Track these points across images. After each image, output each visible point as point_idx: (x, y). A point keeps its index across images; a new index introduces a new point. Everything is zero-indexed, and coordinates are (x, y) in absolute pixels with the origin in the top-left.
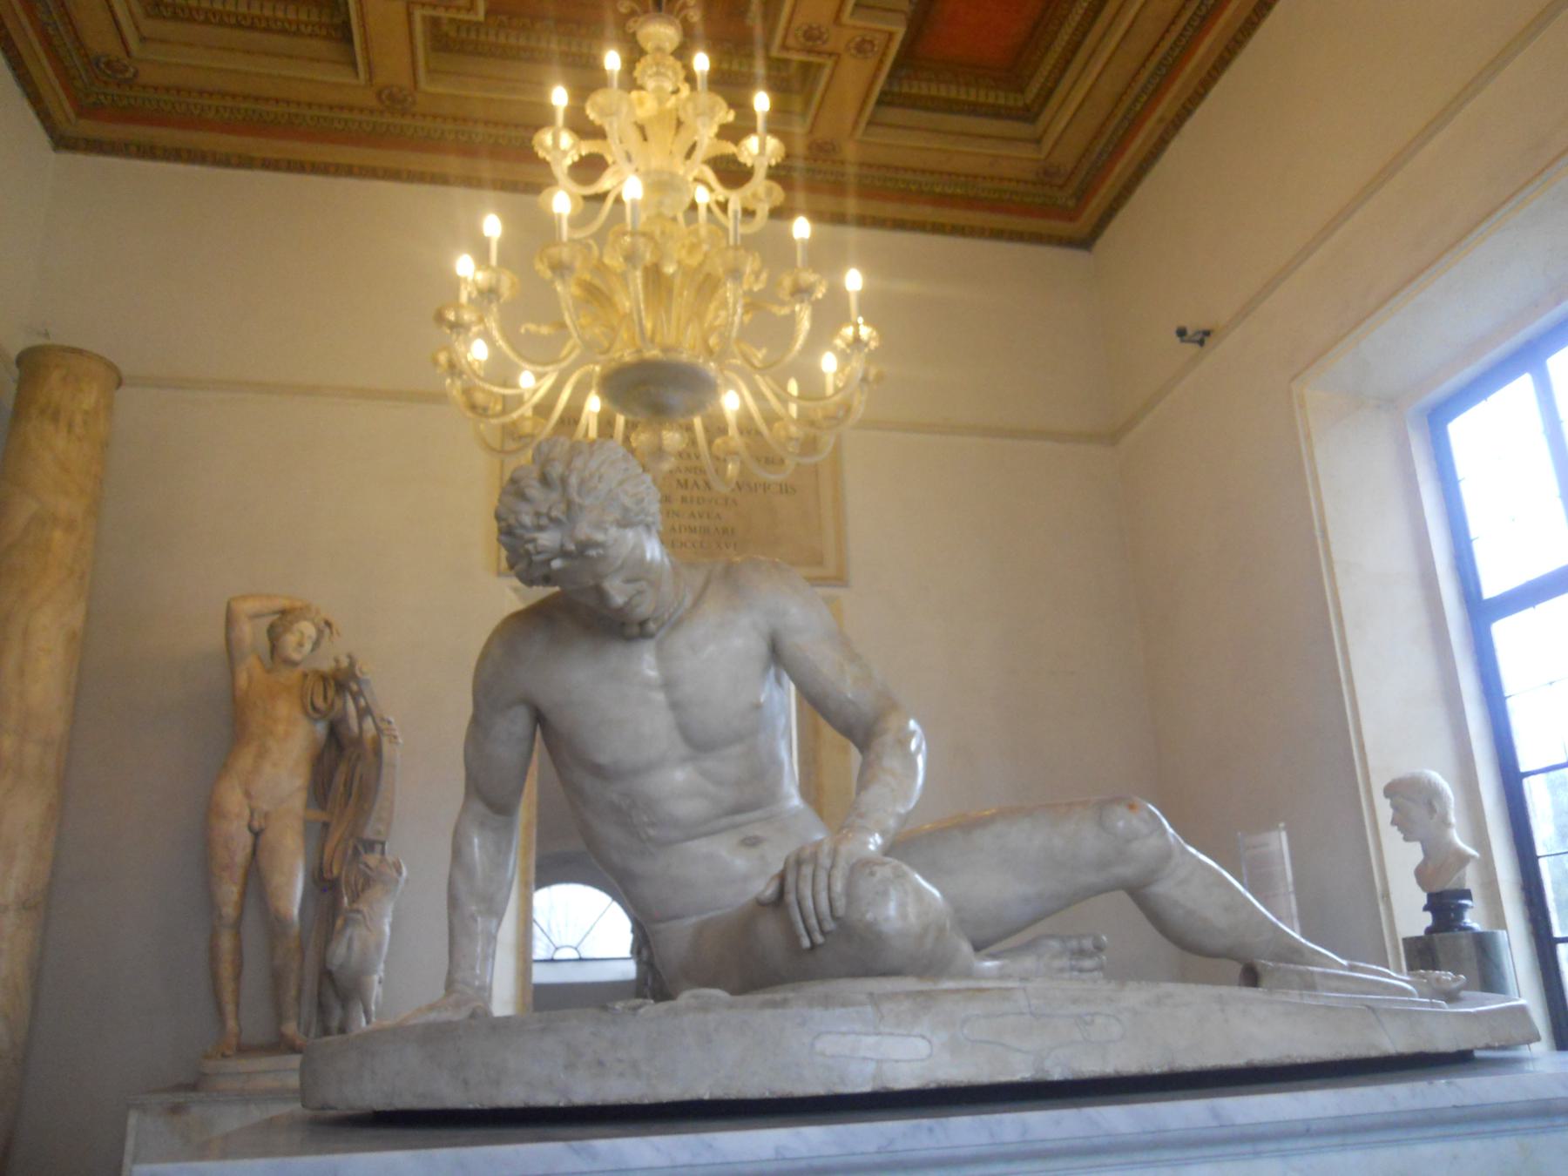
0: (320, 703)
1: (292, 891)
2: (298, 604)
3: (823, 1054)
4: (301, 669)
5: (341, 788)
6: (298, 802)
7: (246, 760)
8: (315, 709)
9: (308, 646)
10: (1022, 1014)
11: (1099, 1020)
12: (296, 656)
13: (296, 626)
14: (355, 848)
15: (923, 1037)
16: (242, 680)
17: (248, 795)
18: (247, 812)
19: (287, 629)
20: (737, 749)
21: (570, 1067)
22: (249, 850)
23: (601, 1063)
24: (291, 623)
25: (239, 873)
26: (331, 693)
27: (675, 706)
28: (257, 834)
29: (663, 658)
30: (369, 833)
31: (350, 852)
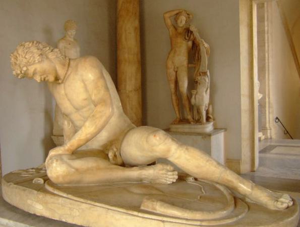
0: (187, 38)
1: (184, 85)
2: (181, 11)
4: (185, 27)
6: (185, 63)
7: (172, 54)
8: (186, 39)
11: (75, 210)
12: (181, 25)
15: (42, 204)
16: (171, 34)
17: (173, 63)
18: (173, 67)
20: (85, 109)
22: (175, 76)
25: (173, 81)
26: (189, 34)
28: (176, 72)
29: (65, 89)
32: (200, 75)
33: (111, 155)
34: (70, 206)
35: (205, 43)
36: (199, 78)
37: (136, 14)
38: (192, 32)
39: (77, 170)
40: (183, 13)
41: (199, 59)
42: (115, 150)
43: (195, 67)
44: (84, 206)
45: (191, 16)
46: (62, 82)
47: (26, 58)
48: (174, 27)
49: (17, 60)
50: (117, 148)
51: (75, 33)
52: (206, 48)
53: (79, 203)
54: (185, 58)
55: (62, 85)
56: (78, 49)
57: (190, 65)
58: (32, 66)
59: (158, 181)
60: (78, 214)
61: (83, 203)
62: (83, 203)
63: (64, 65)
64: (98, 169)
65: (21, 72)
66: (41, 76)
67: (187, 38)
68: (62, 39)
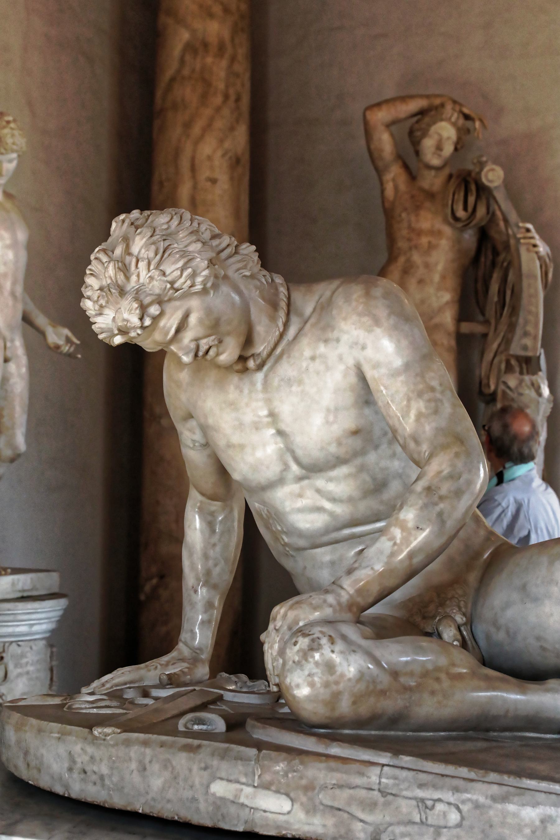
0: (461, 213)
2: (437, 101)
3: (214, 795)
5: (496, 299)
8: (456, 219)
9: (448, 149)
10: (371, 789)
11: (440, 807)
12: (436, 162)
13: (433, 129)
14: (508, 362)
15: (287, 795)
19: (425, 133)
21: (70, 770)
23: (85, 772)
24: (429, 125)
26: (471, 199)
27: (280, 433)
30: (515, 349)
31: (503, 366)
32: (509, 369)
34: (420, 793)
35: (538, 241)
36: (512, 382)
37: (238, 100)
38: (483, 191)
39: (395, 674)
40: (449, 107)
41: (511, 302)
42: (460, 619)
43: (485, 336)
44: (479, 793)
45: (477, 124)
46: (260, 367)
47: (164, 274)
48: (406, 167)
49: (128, 278)
50: (464, 615)
51: (12, 166)
52: (540, 258)
53: (461, 783)
54: (447, 297)
55: (259, 376)
56: (22, 236)
57: (466, 327)
58: (177, 303)
60: (454, 817)
61: (472, 780)
62: (472, 780)
65: (141, 319)
66: (197, 340)
67: (461, 213)
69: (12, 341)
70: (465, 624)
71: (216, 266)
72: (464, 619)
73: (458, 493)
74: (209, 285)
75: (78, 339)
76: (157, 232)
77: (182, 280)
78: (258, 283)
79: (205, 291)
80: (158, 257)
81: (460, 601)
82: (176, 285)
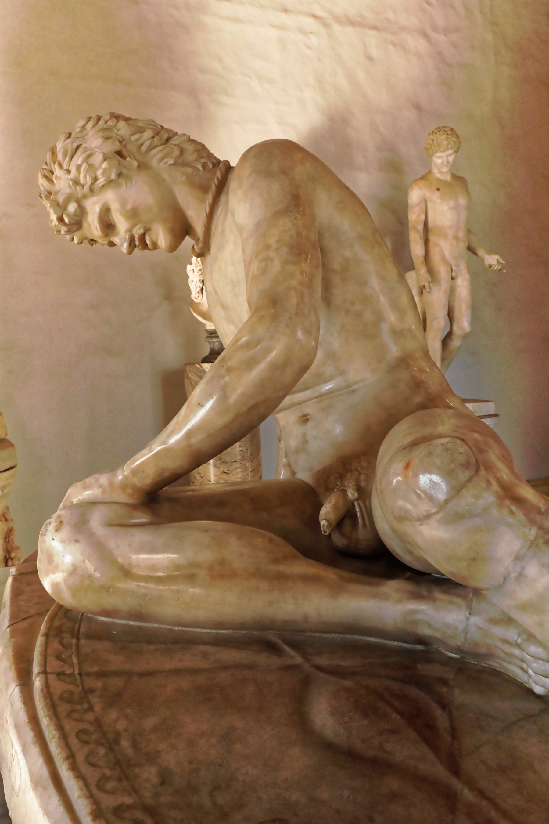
33: (327, 512)
42: (351, 494)
50: (359, 489)
51: (451, 159)
58: (94, 199)
59: (493, 664)
63: (205, 189)
64: (221, 572)
68: (423, 178)
69: (458, 266)
70: (357, 499)
71: (128, 159)
72: (356, 494)
73: (250, 363)
74: (113, 177)
75: (504, 261)
76: (73, 136)
77: (82, 175)
78: (189, 170)
79: (109, 183)
80: (67, 158)
81: (360, 474)
82: (82, 181)
